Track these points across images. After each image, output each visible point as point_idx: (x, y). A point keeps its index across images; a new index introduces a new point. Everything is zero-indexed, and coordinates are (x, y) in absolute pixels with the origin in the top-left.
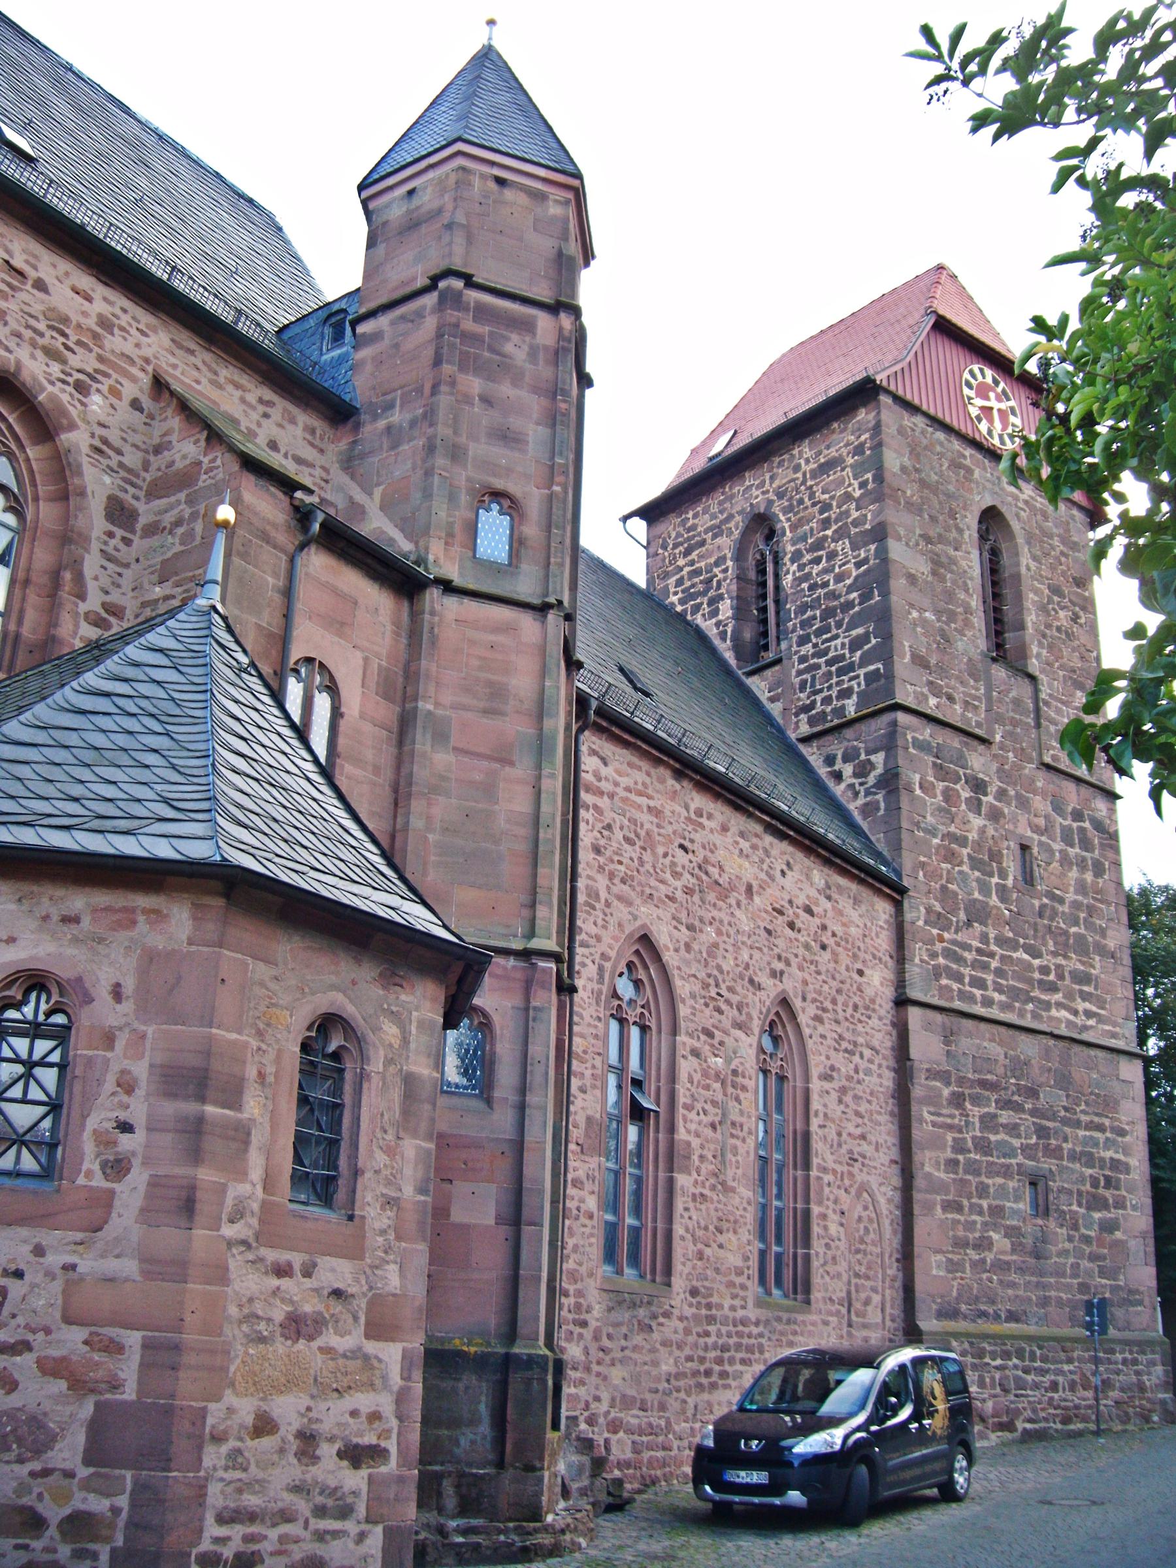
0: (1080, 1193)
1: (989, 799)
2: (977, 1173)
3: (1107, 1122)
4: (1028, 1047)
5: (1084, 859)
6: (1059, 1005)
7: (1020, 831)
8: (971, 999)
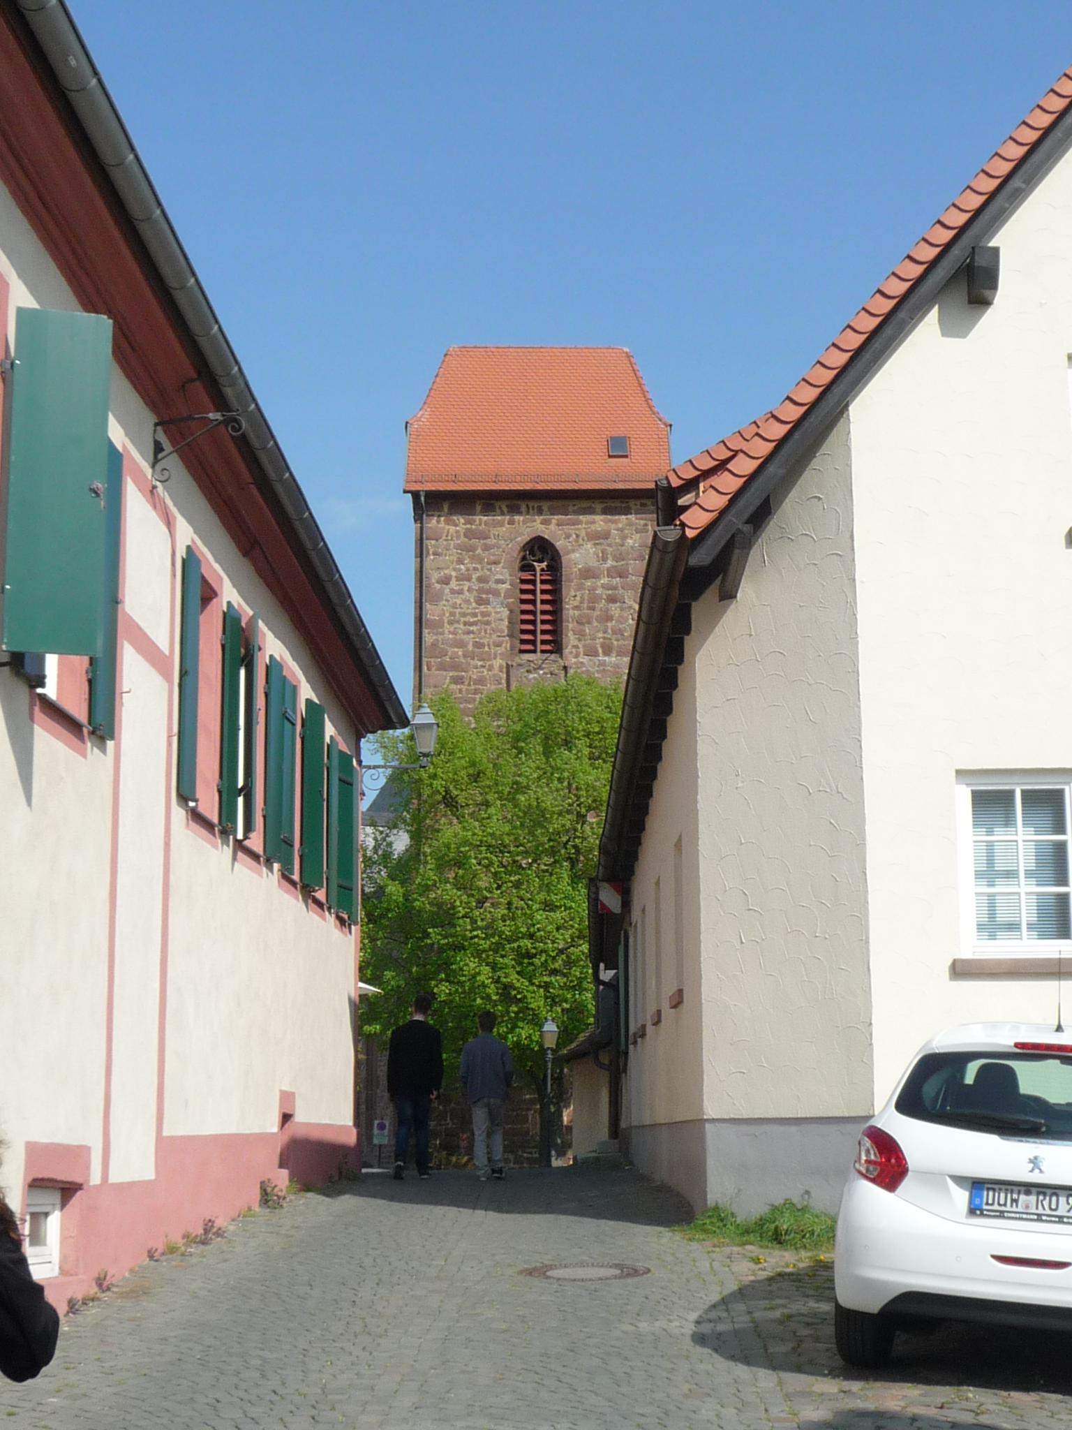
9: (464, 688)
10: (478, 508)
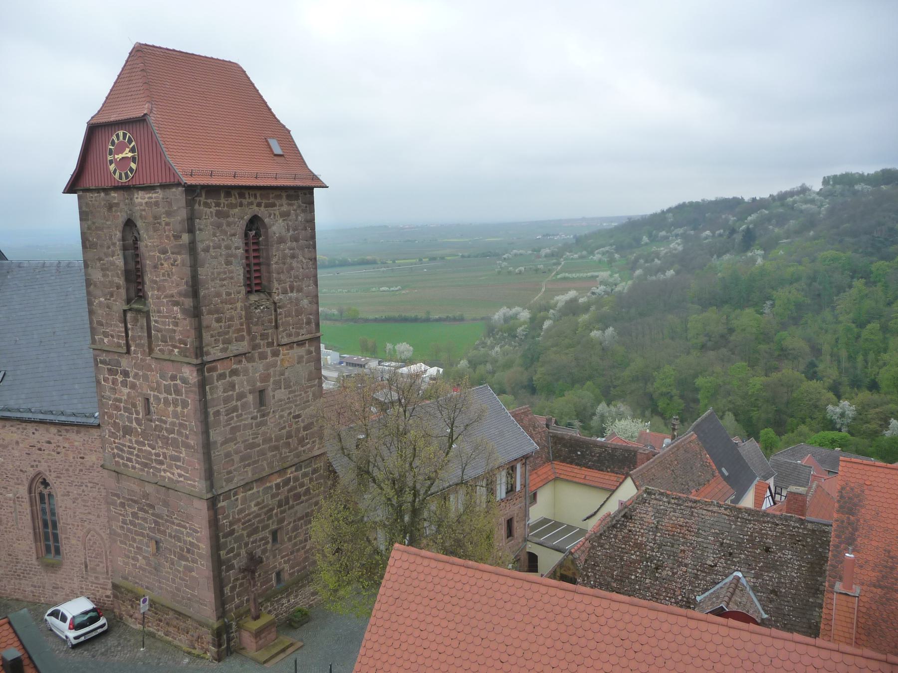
0: (175, 552)
1: (131, 379)
2: (131, 533)
3: (188, 525)
4: (149, 489)
5: (177, 400)
6: (165, 471)
7: (145, 392)
8: (126, 466)
9: (223, 324)
10: (222, 195)
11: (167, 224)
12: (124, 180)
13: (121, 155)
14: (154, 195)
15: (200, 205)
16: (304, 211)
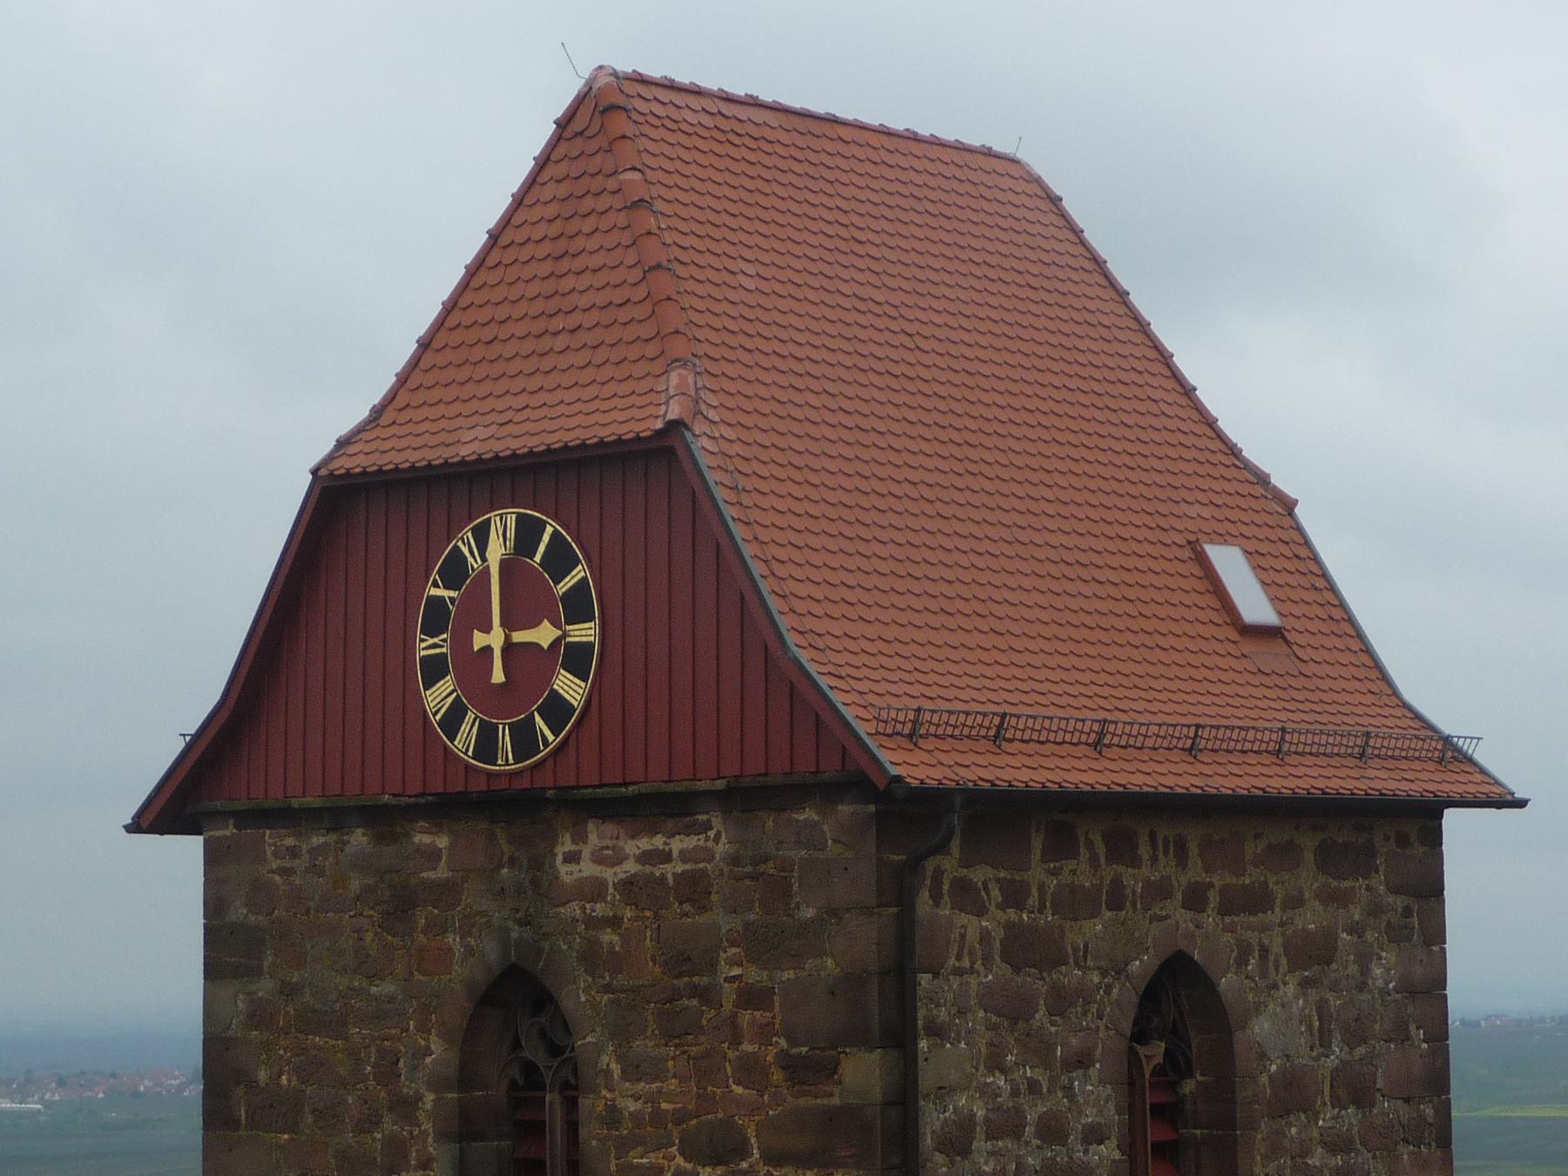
10: (1037, 842)
11: (753, 997)
12: (506, 759)
13: (505, 635)
14: (678, 844)
15: (936, 898)
16: (1397, 935)
